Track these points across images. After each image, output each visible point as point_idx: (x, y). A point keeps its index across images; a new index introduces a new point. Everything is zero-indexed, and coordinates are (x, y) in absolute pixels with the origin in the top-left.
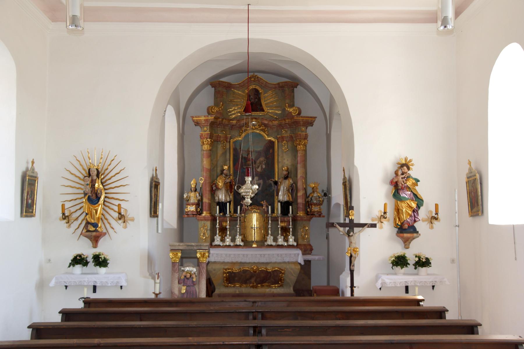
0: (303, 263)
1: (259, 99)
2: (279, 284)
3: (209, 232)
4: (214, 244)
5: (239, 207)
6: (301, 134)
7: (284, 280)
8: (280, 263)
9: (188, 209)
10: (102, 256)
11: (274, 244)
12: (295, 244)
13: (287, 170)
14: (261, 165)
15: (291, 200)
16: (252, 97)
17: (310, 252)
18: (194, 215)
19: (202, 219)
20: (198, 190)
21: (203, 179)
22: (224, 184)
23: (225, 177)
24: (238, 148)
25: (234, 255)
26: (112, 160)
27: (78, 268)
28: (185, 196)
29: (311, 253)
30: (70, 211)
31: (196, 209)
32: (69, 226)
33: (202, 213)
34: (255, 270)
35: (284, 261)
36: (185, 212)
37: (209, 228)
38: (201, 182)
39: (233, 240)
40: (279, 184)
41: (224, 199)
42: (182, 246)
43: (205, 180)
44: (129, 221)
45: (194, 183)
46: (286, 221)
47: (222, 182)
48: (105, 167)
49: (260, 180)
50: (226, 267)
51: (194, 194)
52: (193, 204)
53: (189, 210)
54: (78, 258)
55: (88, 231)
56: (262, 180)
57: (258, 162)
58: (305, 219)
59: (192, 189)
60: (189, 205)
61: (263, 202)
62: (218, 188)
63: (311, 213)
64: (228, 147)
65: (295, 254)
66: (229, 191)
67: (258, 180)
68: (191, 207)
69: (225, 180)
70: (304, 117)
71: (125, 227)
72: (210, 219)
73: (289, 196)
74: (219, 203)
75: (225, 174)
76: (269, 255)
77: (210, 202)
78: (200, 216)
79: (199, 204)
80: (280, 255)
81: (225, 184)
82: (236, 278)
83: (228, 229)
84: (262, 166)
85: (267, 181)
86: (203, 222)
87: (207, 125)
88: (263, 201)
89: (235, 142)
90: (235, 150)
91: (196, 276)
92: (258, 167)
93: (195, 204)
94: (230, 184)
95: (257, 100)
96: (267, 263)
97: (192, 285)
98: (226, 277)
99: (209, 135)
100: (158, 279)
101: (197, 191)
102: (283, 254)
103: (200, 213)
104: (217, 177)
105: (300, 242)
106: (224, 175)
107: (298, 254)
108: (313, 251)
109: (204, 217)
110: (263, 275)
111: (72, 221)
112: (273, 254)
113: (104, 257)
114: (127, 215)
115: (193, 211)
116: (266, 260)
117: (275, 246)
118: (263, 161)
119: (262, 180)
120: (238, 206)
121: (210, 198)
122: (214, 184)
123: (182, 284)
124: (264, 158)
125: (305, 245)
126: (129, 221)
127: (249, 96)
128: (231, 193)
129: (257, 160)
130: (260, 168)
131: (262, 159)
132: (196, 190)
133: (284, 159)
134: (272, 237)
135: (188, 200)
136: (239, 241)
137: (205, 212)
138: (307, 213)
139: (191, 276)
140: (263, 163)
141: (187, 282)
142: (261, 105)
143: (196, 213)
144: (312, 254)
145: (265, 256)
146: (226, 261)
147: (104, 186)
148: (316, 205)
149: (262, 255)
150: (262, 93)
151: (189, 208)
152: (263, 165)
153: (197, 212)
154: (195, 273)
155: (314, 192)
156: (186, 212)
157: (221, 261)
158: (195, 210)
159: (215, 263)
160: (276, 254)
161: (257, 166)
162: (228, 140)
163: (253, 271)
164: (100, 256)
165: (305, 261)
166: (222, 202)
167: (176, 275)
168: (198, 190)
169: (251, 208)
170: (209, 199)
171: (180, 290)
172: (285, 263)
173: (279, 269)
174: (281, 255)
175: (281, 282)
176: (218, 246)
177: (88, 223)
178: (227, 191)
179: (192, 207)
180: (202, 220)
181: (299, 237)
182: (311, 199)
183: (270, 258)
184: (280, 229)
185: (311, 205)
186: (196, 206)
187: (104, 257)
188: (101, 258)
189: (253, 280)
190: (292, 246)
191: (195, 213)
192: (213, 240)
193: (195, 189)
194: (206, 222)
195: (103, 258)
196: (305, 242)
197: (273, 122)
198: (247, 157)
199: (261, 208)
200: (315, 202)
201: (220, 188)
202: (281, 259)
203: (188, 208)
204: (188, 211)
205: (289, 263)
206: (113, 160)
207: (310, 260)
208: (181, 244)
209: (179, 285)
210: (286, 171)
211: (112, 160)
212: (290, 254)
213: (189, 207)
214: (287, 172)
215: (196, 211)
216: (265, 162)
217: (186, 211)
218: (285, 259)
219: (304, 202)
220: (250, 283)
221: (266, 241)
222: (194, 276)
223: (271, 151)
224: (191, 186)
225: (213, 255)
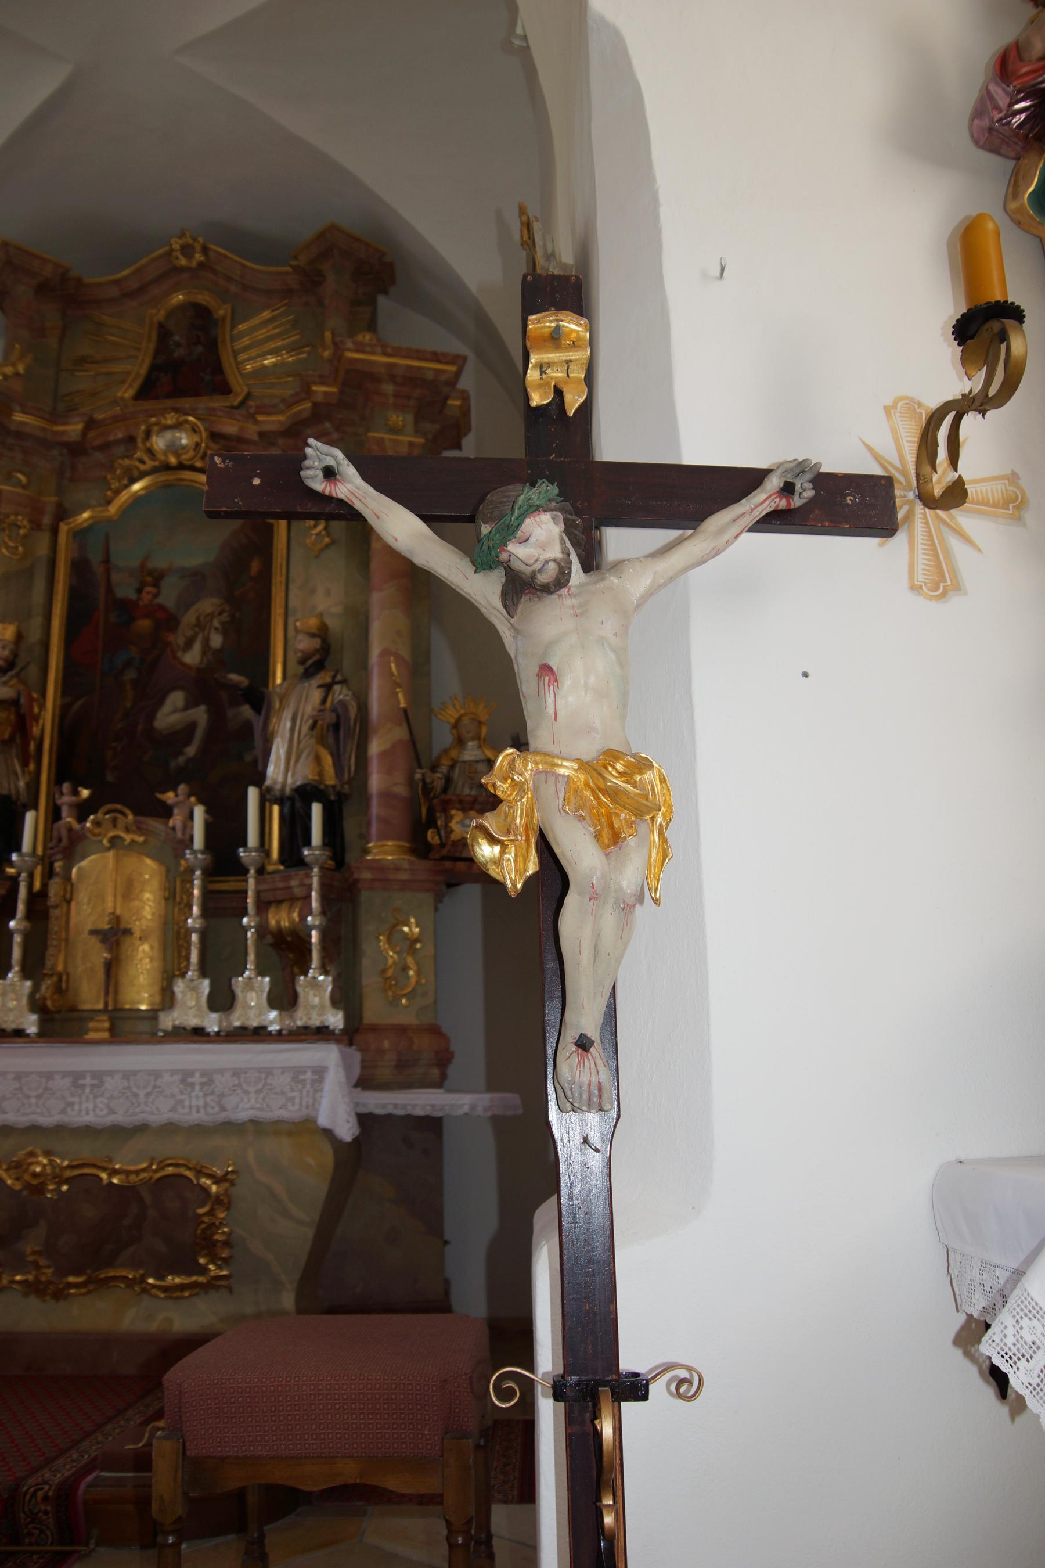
0: (346, 1130)
1: (213, 346)
2: (203, 1271)
6: (387, 443)
7: (227, 1243)
8: (199, 1130)
11: (212, 1023)
12: (335, 1020)
13: (322, 633)
14: (200, 636)
15: (330, 779)
16: (177, 338)
17: (435, 1072)
24: (95, 558)
29: (444, 1076)
34: (35, 1175)
35: (222, 1117)
40: (277, 705)
46: (298, 899)
49: (196, 704)
56: (203, 708)
57: (189, 618)
58: (404, 876)
63: (445, 852)
64: (42, 549)
65: (296, 1072)
67: (186, 708)
70: (398, 352)
73: (318, 759)
76: (127, 1075)
84: (206, 641)
85: (230, 713)
88: (175, 789)
89: (80, 535)
90: (80, 567)
92: (189, 644)
95: (199, 349)
96: (119, 1133)
102: (221, 1071)
105: (374, 1010)
107: (320, 1072)
108: (452, 1070)
112: (157, 1074)
118: (211, 616)
119: (203, 708)
124: (216, 601)
125: (402, 1030)
127: (164, 333)
129: (188, 607)
130: (197, 647)
131: (208, 605)
133: (313, 591)
138: (420, 848)
140: (216, 623)
142: (218, 368)
144: (446, 1083)
145: (102, 1083)
148: (471, 809)
150: (224, 319)
152: (213, 631)
155: (460, 742)
160: (173, 1072)
161: (181, 641)
162: (47, 520)
165: (365, 1120)
172: (229, 1127)
174: (209, 1077)
181: (369, 980)
182: (448, 780)
183: (136, 1095)
185: (446, 806)
190: (321, 1034)
196: (405, 1014)
197: (260, 418)
198: (133, 596)
199: (154, 824)
200: (467, 791)
202: (206, 1105)
205: (257, 1127)
207: (437, 1114)
210: (313, 635)
212: (269, 1072)
214: (316, 643)
216: (225, 617)
218: (231, 1102)
219: (402, 790)
223: (255, 566)
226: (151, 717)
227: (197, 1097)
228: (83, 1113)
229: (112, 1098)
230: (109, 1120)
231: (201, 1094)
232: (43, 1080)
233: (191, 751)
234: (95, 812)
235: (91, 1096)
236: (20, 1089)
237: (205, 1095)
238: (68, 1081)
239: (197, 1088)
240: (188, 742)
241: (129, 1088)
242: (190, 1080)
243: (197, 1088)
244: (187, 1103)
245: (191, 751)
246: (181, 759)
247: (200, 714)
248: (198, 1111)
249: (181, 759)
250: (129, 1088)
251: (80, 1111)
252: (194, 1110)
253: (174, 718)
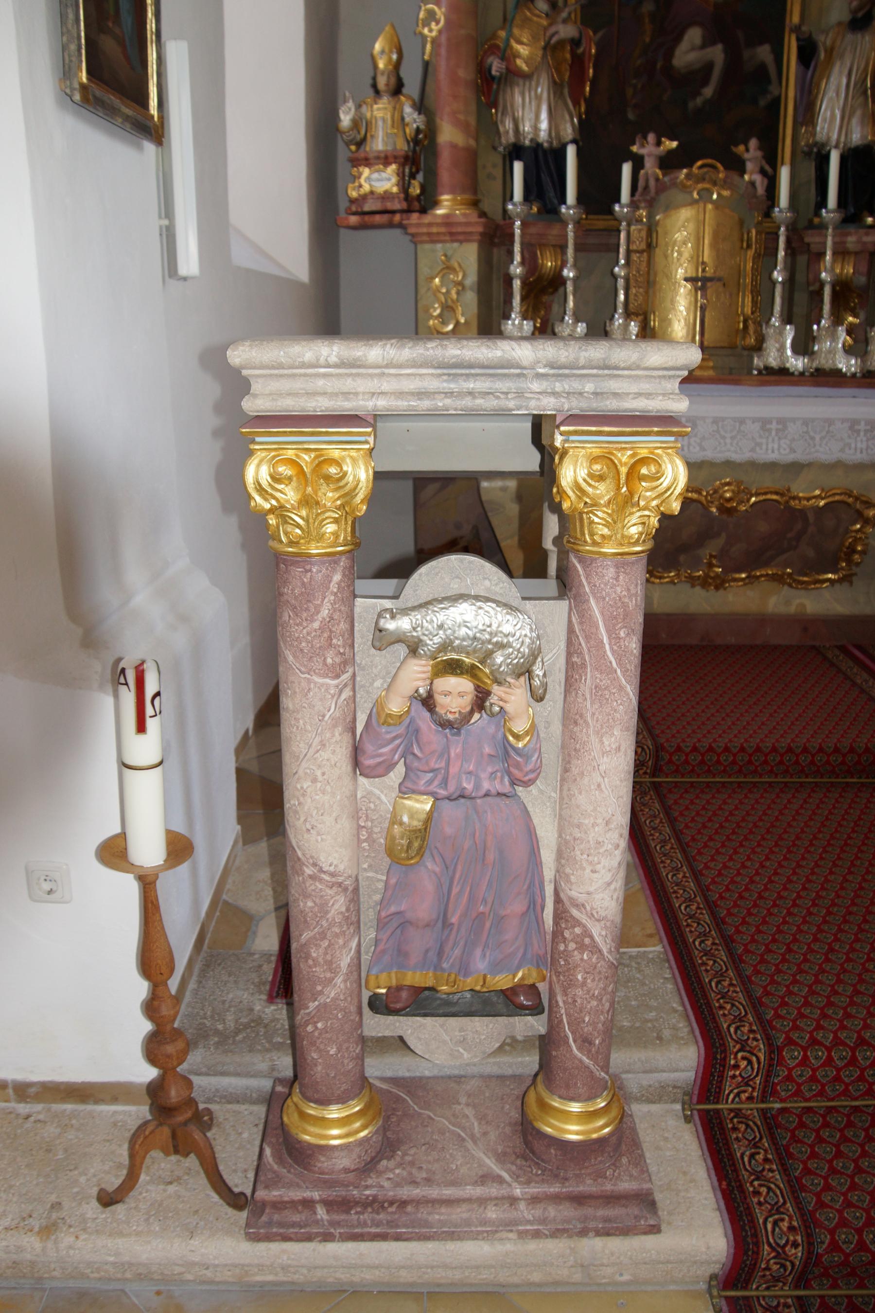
3: (471, 298)
5: (626, 169)
7: (863, 553)
9: (360, 186)
11: (797, 363)
18: (393, 212)
19: (434, 230)
20: (412, 87)
22: (545, 48)
28: (345, 119)
31: (404, 187)
33: (436, 204)
34: (729, 500)
36: (343, 205)
37: (472, 278)
38: (426, 31)
41: (544, 125)
45: (387, 50)
47: (535, 38)
51: (390, 107)
52: (386, 160)
53: (366, 188)
56: (719, 47)
59: (382, 82)
60: (367, 162)
61: (741, 148)
62: (512, 75)
66: (566, 91)
68: (375, 176)
69: (553, 30)
72: (480, 229)
74: (516, 151)
76: (806, 422)
77: (472, 142)
78: (427, 219)
80: (862, 426)
81: (551, 49)
83: (570, 287)
86: (439, 246)
88: (746, 144)
94: (573, 53)
96: (795, 468)
101: (405, 90)
109: (448, 221)
110: (763, 527)
115: (386, 196)
116: (793, 451)
117: (802, 374)
119: (719, 47)
120: (626, 161)
121: (472, 120)
122: (494, 49)
128: (576, 103)
132: (397, 89)
134: (789, 332)
135: (360, 143)
137: (446, 198)
143: (404, 205)
145: (785, 428)
149: (774, 426)
151: (368, 179)
153: (407, 197)
156: (352, 201)
158: (395, 190)
163: (722, 509)
166: (537, 146)
168: (412, 87)
169: (688, 176)
170: (464, 127)
173: (850, 500)
175: (849, 562)
178: (556, 87)
179: (384, 175)
180: (433, 239)
183: (813, 438)
184: (827, 291)
186: (403, 165)
191: (397, 205)
193: (393, 80)
194: (456, 245)
201: (525, 67)
202: (868, 447)
203: (362, 180)
204: (364, 198)
213: (366, 172)
215: (402, 196)
217: (354, 194)
221: (759, 347)
224: (375, 66)
226: (669, 55)
227: (862, 441)
228: (770, 451)
229: (793, 440)
230: (791, 458)
231: (864, 439)
232: (738, 424)
233: (708, 92)
234: (690, 165)
235: (776, 438)
236: (718, 431)
237: (868, 440)
239: (862, 434)
240: (705, 82)
241: (807, 432)
242: (857, 427)
243: (862, 434)
244: (853, 446)
245: (708, 92)
246: (699, 101)
247: (717, 53)
248: (861, 452)
249: (699, 101)
250: (807, 432)
251: (767, 449)
252: (858, 451)
253: (692, 57)
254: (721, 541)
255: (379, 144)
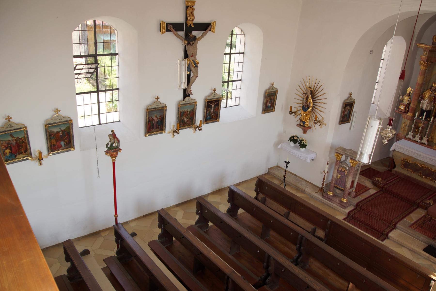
4: (407, 137)
10: (303, 142)
21: (413, 90)
23: (432, 92)
25: (412, 152)
26: (321, 86)
27: (292, 144)
30: (297, 109)
31: (405, 109)
32: (296, 117)
33: (407, 113)
34: (423, 166)
37: (408, 125)
39: (421, 139)
42: (342, 152)
43: (414, 91)
44: (323, 125)
48: (317, 89)
50: (404, 157)
52: (404, 105)
54: (292, 138)
55: (300, 125)
59: (407, 94)
60: (401, 105)
68: (402, 106)
71: (321, 128)
75: (432, 90)
79: (407, 106)
82: (410, 167)
87: (427, 51)
91: (347, 172)
93: (405, 105)
96: (433, 166)
97: (344, 176)
98: (403, 163)
99: (426, 59)
100: (327, 165)
103: (406, 112)
104: (427, 90)
106: (431, 90)
111: (298, 115)
113: (304, 143)
114: (323, 121)
115: (402, 110)
116: (433, 163)
123: (339, 173)
126: (323, 125)
136: (425, 139)
139: (344, 171)
141: (342, 173)
143: (404, 112)
145: (433, 160)
146: (405, 153)
147: (313, 101)
149: (431, 159)
154: (347, 170)
157: (402, 152)
159: (398, 152)
164: (302, 141)
166: (423, 109)
167: (337, 167)
171: (337, 176)
176: (409, 139)
177: (301, 120)
187: (304, 143)
188: (302, 142)
189: (421, 172)
191: (403, 111)
192: (407, 134)
195: (303, 143)
204: (400, 109)
206: (321, 86)
208: (342, 151)
209: (338, 173)
211: (321, 86)
220: (419, 173)
222: (346, 172)
225: (398, 147)
230: (433, 164)
238: (429, 159)
254: (422, 171)
255: (404, 102)
